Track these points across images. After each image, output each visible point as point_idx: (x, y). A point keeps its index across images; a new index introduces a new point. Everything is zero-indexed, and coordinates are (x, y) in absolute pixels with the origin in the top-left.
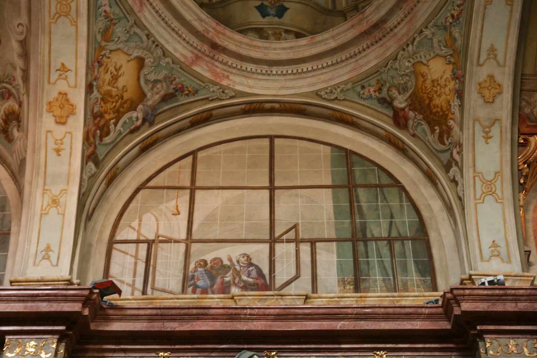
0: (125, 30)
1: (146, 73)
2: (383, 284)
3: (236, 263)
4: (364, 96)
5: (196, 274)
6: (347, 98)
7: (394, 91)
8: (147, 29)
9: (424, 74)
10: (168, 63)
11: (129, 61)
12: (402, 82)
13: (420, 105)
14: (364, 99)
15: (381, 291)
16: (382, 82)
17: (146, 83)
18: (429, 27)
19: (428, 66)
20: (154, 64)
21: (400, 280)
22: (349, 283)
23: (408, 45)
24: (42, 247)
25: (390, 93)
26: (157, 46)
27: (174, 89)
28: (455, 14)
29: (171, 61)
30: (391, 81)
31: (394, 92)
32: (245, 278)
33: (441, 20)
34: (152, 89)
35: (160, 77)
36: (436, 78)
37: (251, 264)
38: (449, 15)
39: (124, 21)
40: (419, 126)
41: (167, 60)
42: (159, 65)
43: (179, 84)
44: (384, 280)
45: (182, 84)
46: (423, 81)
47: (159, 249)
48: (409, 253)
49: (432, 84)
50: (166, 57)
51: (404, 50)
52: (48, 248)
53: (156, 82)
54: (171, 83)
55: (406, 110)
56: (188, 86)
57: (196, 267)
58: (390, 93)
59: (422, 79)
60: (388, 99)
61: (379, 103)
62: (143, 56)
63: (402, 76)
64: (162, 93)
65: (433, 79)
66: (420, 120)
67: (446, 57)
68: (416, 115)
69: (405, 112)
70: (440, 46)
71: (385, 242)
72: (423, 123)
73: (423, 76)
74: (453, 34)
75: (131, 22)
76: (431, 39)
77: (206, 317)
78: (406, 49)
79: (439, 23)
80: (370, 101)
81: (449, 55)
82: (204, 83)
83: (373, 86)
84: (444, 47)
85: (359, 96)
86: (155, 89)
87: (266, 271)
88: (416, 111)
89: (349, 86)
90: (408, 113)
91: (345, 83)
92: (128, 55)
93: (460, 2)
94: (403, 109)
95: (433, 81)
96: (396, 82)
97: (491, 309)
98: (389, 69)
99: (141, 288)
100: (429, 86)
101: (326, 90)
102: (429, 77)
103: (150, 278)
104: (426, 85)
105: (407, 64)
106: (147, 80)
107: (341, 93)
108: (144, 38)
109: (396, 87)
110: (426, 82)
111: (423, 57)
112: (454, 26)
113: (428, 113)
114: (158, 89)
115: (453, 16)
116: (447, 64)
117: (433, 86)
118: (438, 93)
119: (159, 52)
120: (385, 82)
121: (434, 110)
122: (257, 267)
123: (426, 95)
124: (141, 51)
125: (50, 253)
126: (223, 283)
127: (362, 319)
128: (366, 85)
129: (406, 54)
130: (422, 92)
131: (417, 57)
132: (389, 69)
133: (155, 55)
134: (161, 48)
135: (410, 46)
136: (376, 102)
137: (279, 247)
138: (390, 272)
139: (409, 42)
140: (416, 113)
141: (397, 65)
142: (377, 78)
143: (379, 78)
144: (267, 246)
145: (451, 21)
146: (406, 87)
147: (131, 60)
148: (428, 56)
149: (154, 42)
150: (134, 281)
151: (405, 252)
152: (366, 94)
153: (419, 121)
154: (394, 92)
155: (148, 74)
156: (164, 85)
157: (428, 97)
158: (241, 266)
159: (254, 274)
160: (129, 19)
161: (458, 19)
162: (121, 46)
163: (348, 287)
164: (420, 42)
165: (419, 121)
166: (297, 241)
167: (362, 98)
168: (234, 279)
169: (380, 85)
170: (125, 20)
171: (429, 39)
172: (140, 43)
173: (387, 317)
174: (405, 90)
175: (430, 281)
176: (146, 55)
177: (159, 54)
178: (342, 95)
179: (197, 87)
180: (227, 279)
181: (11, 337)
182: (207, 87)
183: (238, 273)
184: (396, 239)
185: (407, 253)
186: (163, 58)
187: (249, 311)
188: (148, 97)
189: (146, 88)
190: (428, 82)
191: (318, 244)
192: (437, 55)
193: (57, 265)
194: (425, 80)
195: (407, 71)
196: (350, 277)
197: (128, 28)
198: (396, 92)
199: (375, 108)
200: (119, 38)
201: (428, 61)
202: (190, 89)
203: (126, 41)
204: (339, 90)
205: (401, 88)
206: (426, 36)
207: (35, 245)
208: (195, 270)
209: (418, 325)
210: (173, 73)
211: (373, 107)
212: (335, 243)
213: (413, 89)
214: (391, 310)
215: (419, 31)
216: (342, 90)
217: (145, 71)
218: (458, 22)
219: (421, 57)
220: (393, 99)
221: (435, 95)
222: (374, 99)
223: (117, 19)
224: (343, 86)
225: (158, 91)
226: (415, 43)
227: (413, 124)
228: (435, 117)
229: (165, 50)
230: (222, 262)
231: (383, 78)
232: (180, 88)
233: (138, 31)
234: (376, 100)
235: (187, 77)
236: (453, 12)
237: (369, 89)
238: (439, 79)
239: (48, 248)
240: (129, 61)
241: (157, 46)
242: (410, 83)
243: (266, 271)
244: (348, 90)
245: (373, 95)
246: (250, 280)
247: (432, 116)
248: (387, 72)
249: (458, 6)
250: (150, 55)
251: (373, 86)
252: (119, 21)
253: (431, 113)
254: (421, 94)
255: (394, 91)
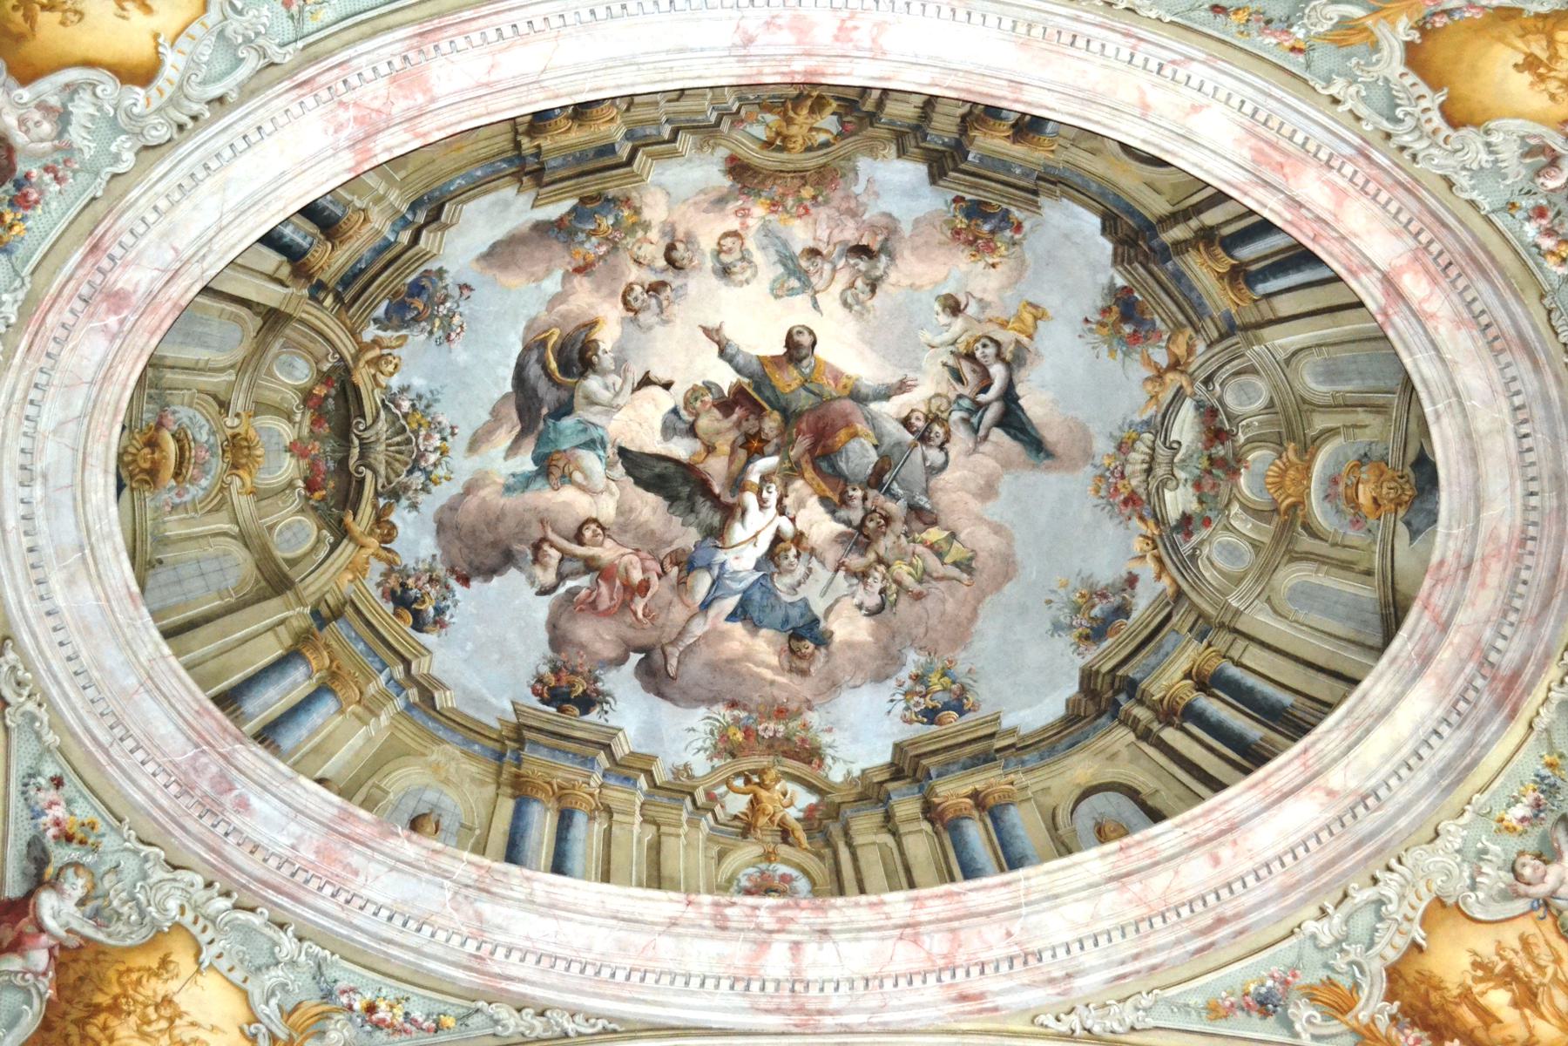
0: (258, 34)
1: (99, 91)
4: (32, 793)
6: (14, 735)
7: (80, 882)
8: (240, 103)
9: (172, 966)
10: (117, 158)
11: (156, 36)
12: (115, 903)
13: (81, 979)
14: (23, 793)
16: (91, 841)
17: (67, 85)
18: (306, 944)
19: (198, 971)
20: (122, 119)
23: (227, 894)
25: (70, 872)
26: (181, 127)
27: (27, 176)
28: (380, 1015)
29: (121, 168)
30: (104, 868)
31: (76, 886)
33: (343, 974)
34: (43, 107)
35: (75, 134)
36: (183, 1008)
38: (369, 996)
39: (287, 29)
40: (20, 997)
41: (129, 158)
42: (116, 128)
43: (41, 193)
45: (37, 202)
46: (150, 969)
49: (159, 999)
50: (137, 154)
51: (209, 885)
53: (62, 118)
54: (47, 169)
55: (44, 938)
56: (29, 223)
58: (70, 872)
59: (155, 965)
60: (50, 871)
61: (29, 845)
62: (160, 82)
63: (133, 898)
64: (19, 138)
65: (176, 999)
66: (41, 995)
67: (259, 1021)
68: (45, 974)
69: (35, 936)
70: (273, 994)
72: (36, 1001)
73: (164, 963)
74: (330, 1025)
75: (276, 54)
76: (277, 963)
78: (214, 892)
79: (331, 974)
80: (26, 813)
81: (270, 1031)
82: (33, 273)
83: (72, 814)
84: (280, 1007)
85: (31, 776)
86: (37, 116)
88: (57, 971)
89: (51, 738)
90: (36, 948)
91: (58, 724)
92: (178, 35)
93: (420, 1020)
94: (41, 929)
95: (167, 1000)
96: (107, 883)
98: (136, 852)
100: (150, 993)
101: (21, 666)
102: (173, 986)
104: (144, 980)
105: (173, 905)
106: (75, 91)
107: (23, 714)
108: (215, 91)
109: (94, 886)
110: (153, 980)
111: (215, 949)
112: (350, 1020)
113: (76, 1013)
114: (37, 124)
115: (371, 1009)
116: (242, 1030)
117: (157, 1007)
118: (146, 1028)
119: (161, 133)
120: (95, 849)
121: (93, 1031)
123: (116, 990)
124: (176, 80)
128: (67, 790)
129: (200, 894)
130: (121, 974)
131: (204, 929)
132: (136, 852)
133: (154, 120)
134: (169, 140)
135: (223, 903)
136: (27, 835)
139: (235, 895)
140: (51, 974)
141: (158, 874)
142: (99, 820)
143: (101, 827)
145: (357, 1006)
146: (109, 920)
147: (157, 45)
148: (224, 964)
149: (194, 118)
152: (41, 795)
153: (34, 991)
154: (76, 886)
155: (94, 94)
156: (47, 145)
157: (116, 998)
160: (290, 48)
161: (378, 1026)
162: (213, 16)
164: (248, 931)
165: (34, 991)
167: (26, 785)
169: (80, 835)
170: (291, 37)
171: (273, 953)
172: (201, 76)
174: (98, 917)
176: (161, 92)
177: (154, 133)
178: (19, 720)
179: (20, 252)
182: (17, 283)
186: (139, 145)
188: (21, 91)
189: (48, 88)
190: (155, 988)
192: (246, 995)
194: (157, 975)
195: (152, 909)
197: (261, 41)
198: (79, 893)
199: (11, 837)
200: (240, 13)
201: (211, 966)
202: (16, 229)
203: (221, 34)
204: (31, 706)
205: (99, 902)
206: (275, 944)
210: (81, 177)
211: (12, 827)
213: (111, 942)
215: (280, 919)
216: (33, 718)
217: (109, 87)
218: (368, 1028)
219: (211, 942)
220: (54, 884)
221: (133, 1020)
222: (36, 826)
223: (301, 11)
224: (46, 719)
225: (30, 124)
226: (242, 916)
227: (16, 973)
228: (75, 1039)
229: (158, 152)
231: (105, 840)
232: (25, 196)
233: (243, 72)
234: (33, 832)
235: (60, 218)
236: (382, 1005)
237: (57, 804)
238: (187, 1019)
240: (156, 36)
241: (181, 127)
242: (122, 928)
244: (39, 737)
245: (44, 819)
247: (72, 1029)
248: (126, 849)
249: (407, 1014)
250: (153, 106)
251: (72, 814)
252: (292, 17)
253: (81, 1023)
254: (112, 975)
255: (80, 882)
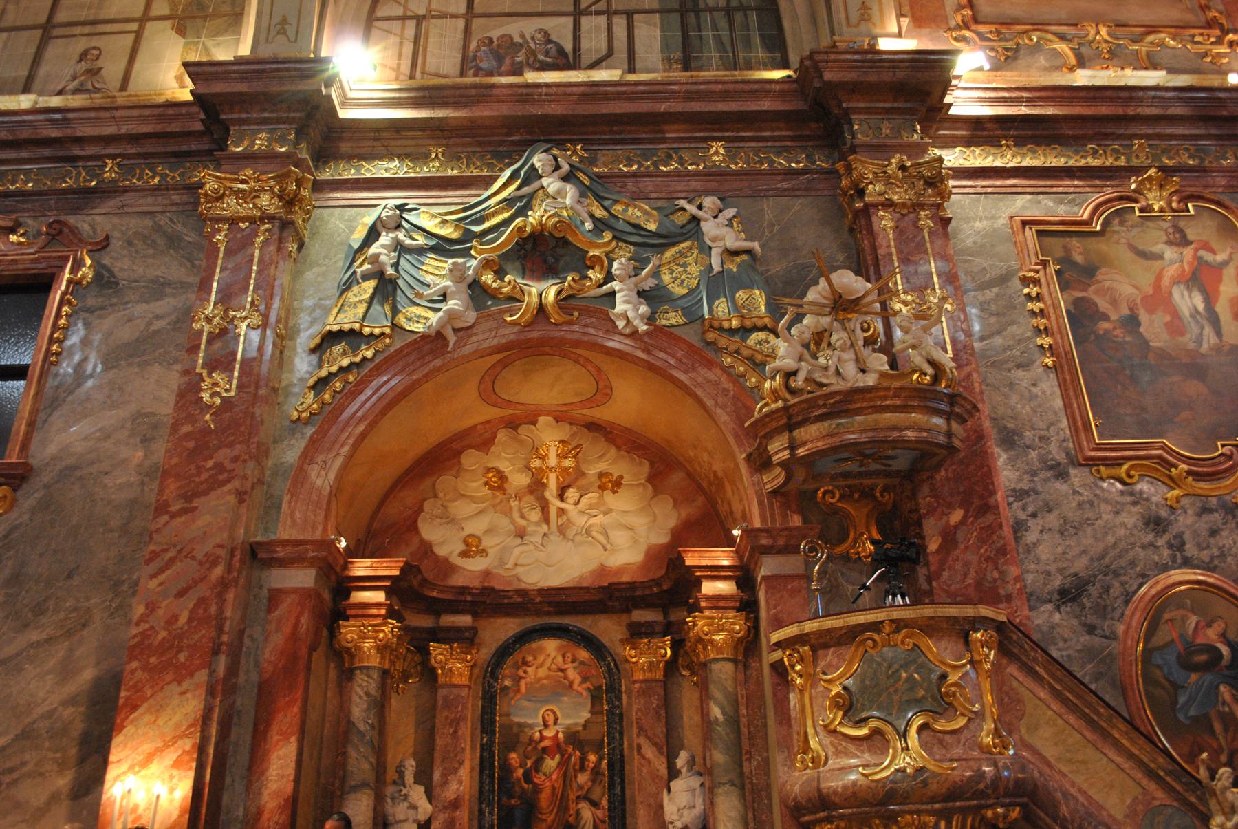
2: (720, 63)
3: (530, 41)
5: (478, 54)
15: (717, 70)
21: (741, 57)
22: (676, 62)
24: (275, 20)
32: (541, 57)
37: (550, 41)
44: (721, 58)
47: (431, 26)
48: (754, 25)
52: (284, 21)
57: (478, 46)
71: (723, 13)
77: (488, 99)
87: (568, 47)
97: (861, 79)
99: (407, 72)
103: (420, 61)
122: (556, 44)
125: (287, 27)
126: (513, 63)
127: (692, 99)
137: (585, 21)
138: (729, 48)
144: (570, 20)
150: (399, 65)
151: (748, 24)
158: (536, 44)
159: (553, 52)
163: (675, 66)
166: (610, 13)
168: (528, 58)
173: (725, 96)
175: (779, 59)
180: (518, 59)
181: (237, 128)
183: (533, 53)
184: (737, 9)
185: (751, 25)
187: (544, 90)
191: (636, 16)
193: (296, 41)
196: (678, 54)
207: (268, 17)
208: (478, 49)
209: (765, 105)
212: (657, 15)
214: (731, 87)
230: (512, 39)
239: (284, 21)
243: (568, 47)
246: (548, 59)
